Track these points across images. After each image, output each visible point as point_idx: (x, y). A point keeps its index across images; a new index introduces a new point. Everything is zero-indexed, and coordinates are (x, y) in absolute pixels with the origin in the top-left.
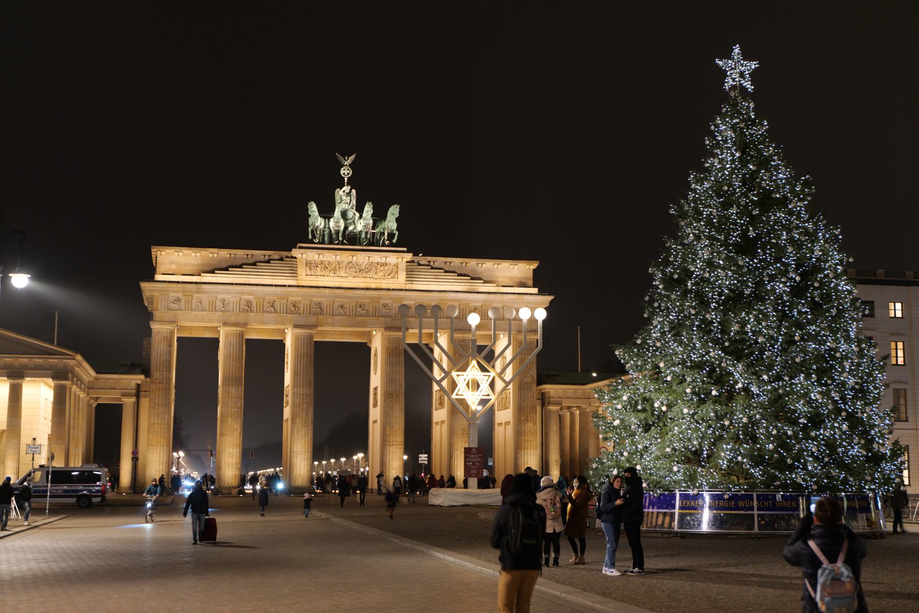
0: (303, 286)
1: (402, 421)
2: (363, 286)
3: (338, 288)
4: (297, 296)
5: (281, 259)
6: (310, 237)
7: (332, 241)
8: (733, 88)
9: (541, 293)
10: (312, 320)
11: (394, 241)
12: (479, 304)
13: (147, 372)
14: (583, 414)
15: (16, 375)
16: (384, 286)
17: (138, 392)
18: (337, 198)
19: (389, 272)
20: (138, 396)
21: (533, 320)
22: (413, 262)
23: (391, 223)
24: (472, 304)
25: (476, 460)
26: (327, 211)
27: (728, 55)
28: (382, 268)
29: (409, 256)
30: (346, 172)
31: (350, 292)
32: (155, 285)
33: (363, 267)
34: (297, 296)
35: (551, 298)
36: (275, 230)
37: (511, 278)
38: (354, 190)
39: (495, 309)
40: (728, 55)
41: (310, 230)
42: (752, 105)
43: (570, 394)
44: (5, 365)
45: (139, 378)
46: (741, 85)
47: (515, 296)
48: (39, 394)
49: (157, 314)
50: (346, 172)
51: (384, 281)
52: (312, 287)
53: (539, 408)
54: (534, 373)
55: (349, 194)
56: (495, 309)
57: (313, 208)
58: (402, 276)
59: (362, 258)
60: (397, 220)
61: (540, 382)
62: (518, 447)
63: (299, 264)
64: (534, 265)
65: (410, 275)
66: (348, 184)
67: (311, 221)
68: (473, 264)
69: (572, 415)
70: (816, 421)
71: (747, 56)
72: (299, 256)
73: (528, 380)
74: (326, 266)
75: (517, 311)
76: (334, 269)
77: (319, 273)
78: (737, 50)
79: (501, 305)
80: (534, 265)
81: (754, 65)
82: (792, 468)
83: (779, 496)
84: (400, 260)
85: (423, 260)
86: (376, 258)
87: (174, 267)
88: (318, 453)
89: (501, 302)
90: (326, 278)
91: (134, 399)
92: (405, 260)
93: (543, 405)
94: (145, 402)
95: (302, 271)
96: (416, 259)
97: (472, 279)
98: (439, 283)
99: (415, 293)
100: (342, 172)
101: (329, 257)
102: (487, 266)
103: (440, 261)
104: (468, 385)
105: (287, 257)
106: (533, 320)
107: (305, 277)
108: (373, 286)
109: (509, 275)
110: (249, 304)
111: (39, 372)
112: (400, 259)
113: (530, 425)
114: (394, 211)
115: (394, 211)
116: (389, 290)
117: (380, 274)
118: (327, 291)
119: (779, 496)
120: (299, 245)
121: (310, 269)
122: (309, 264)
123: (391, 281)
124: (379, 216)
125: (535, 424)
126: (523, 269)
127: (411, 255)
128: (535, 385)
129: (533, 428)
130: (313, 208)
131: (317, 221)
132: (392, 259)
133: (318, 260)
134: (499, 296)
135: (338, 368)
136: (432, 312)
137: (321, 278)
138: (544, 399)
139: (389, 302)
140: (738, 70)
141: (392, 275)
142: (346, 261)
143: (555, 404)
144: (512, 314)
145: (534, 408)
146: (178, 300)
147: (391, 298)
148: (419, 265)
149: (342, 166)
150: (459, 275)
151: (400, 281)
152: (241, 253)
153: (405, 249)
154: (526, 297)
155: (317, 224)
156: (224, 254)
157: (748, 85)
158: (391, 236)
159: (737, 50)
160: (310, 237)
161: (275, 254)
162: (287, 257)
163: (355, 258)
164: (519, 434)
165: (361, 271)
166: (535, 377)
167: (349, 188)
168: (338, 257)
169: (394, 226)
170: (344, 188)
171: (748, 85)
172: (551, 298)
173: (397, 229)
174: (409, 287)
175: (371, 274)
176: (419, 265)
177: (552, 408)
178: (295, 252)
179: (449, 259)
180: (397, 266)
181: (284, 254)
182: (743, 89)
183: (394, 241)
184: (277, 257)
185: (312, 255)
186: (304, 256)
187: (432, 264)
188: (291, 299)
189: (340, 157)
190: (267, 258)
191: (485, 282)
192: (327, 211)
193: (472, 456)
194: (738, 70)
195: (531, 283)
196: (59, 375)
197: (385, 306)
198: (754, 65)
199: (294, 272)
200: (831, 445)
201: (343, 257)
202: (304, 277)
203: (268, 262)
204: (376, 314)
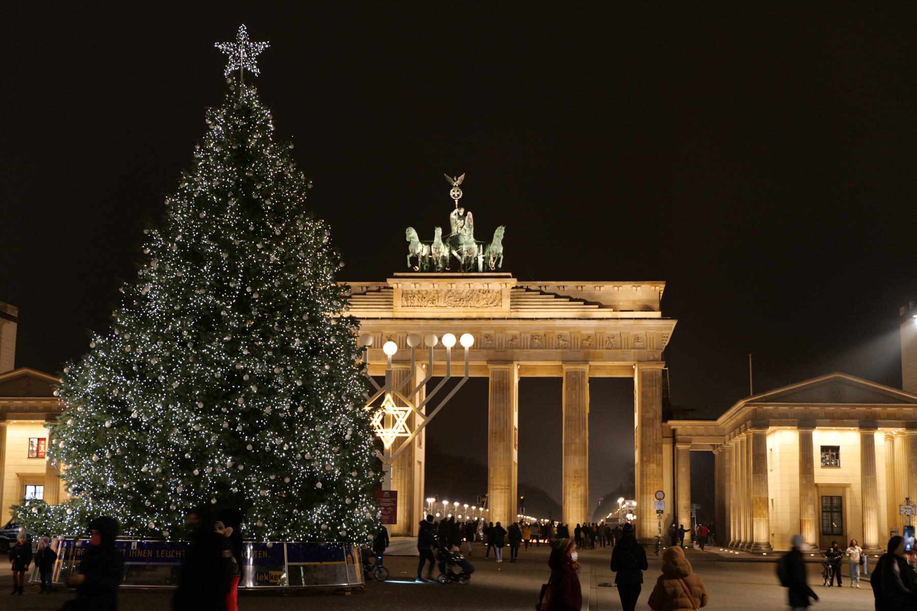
0: (397, 319)
2: (463, 315)
3: (434, 319)
4: (391, 329)
5: (379, 291)
6: (409, 265)
7: (430, 267)
8: (235, 73)
9: (664, 317)
11: (500, 266)
12: (592, 332)
16: (486, 315)
18: (452, 222)
21: (458, 347)
22: (522, 287)
23: (497, 247)
24: (583, 332)
25: (389, 505)
26: (427, 238)
27: (232, 37)
28: (484, 296)
29: (513, 282)
30: (455, 194)
31: (447, 322)
33: (464, 295)
34: (391, 329)
35: (673, 323)
37: (634, 302)
38: (469, 213)
39: (413, 336)
40: (232, 37)
41: (408, 257)
42: (253, 92)
43: (701, 430)
44: (45, 408)
46: (245, 69)
47: (631, 322)
50: (455, 194)
51: (486, 310)
52: (406, 319)
53: (667, 449)
54: (658, 408)
55: (460, 217)
56: (413, 336)
57: (412, 234)
58: (506, 303)
59: (462, 286)
60: (503, 242)
61: (667, 415)
63: (395, 295)
64: (660, 287)
65: (516, 301)
66: (459, 207)
67: (410, 248)
68: (589, 287)
70: (202, 455)
71: (254, 36)
72: (395, 286)
73: (650, 415)
74: (423, 296)
75: (440, 339)
76: (433, 299)
77: (416, 303)
78: (243, 30)
79: (617, 332)
80: (660, 287)
81: (263, 46)
82: (151, 512)
83: (134, 544)
84: (504, 286)
85: (534, 285)
86: (478, 285)
89: (616, 328)
90: (423, 309)
92: (510, 286)
93: (674, 442)
95: (398, 302)
96: (526, 284)
97: (586, 303)
98: (552, 312)
99: (517, 322)
100: (452, 193)
101: (426, 285)
103: (552, 286)
104: (395, 421)
105: (385, 288)
106: (458, 347)
107: (401, 309)
108: (474, 315)
109: (632, 298)
112: (507, 285)
113: (653, 466)
114: (500, 233)
115: (500, 233)
116: (489, 319)
117: (483, 303)
118: (422, 322)
119: (134, 544)
120: (395, 274)
121: (407, 300)
122: (405, 295)
123: (494, 309)
125: (660, 464)
126: (651, 291)
127: (515, 280)
128: (658, 422)
130: (412, 234)
131: (420, 249)
132: (495, 285)
133: (415, 290)
134: (612, 322)
137: (418, 309)
138: (673, 436)
139: (492, 332)
140: (243, 53)
141: (495, 303)
142: (445, 290)
143: (684, 442)
144: (432, 341)
147: (492, 328)
148: (528, 290)
149: (452, 187)
150: (572, 300)
153: (510, 274)
154: (644, 322)
155: (417, 252)
157: (256, 71)
159: (243, 30)
160: (409, 265)
161: (373, 285)
162: (385, 288)
163: (454, 286)
165: (460, 299)
166: (660, 412)
167: (462, 210)
168: (436, 286)
169: (501, 250)
170: (456, 211)
171: (256, 71)
173: (504, 253)
174: (514, 315)
175: (472, 303)
176: (528, 290)
177: (680, 446)
178: (391, 282)
179: (561, 283)
180: (500, 292)
181: (381, 284)
182: (248, 75)
183: (500, 266)
184: (376, 289)
185: (408, 285)
186: (400, 285)
187: (543, 289)
190: (365, 289)
191: (601, 306)
192: (427, 238)
193: (384, 500)
194: (243, 53)
195: (657, 306)
197: (487, 336)
198: (263, 46)
199: (389, 303)
200: (222, 485)
201: (442, 285)
202: (400, 308)
203: (364, 294)
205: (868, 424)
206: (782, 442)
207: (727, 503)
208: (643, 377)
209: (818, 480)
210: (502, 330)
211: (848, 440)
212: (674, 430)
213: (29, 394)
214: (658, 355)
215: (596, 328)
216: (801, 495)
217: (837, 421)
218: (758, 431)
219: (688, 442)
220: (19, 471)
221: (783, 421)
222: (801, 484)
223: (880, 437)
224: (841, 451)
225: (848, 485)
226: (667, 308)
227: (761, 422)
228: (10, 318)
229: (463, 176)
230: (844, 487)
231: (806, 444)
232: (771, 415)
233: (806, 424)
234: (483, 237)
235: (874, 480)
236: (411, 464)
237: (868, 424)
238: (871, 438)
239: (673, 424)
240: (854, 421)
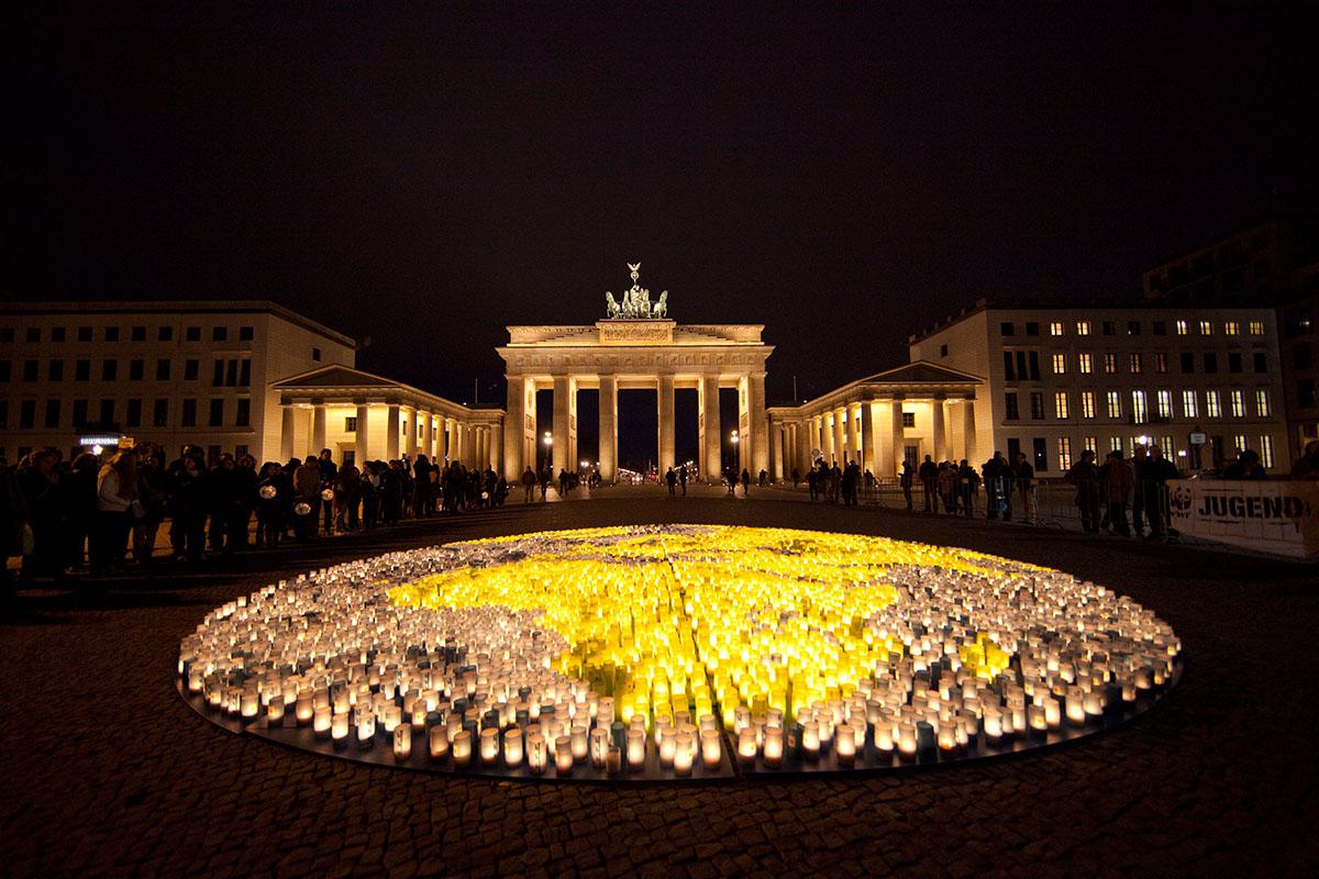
1: (673, 431)
7: (626, 318)
9: (766, 344)
10: (611, 369)
12: (723, 354)
13: (505, 409)
14: (798, 426)
15: (360, 400)
17: (502, 421)
19: (662, 337)
20: (502, 424)
26: (619, 299)
30: (635, 275)
32: (504, 349)
36: (588, 313)
45: (498, 412)
48: (378, 415)
49: (508, 369)
50: (635, 275)
53: (767, 424)
57: (610, 296)
58: (670, 337)
59: (642, 327)
61: (767, 406)
62: (753, 451)
65: (675, 336)
68: (719, 327)
69: (791, 429)
73: (758, 405)
74: (618, 333)
76: (623, 334)
80: (762, 328)
86: (652, 326)
87: (521, 340)
88: (623, 461)
91: (496, 425)
93: (770, 422)
94: (506, 427)
95: (603, 337)
102: (729, 329)
107: (604, 340)
110: (568, 359)
111: (377, 398)
114: (664, 295)
115: (664, 295)
124: (654, 298)
129: (763, 438)
130: (610, 296)
132: (663, 326)
135: (638, 406)
136: (693, 361)
138: (770, 418)
143: (778, 420)
145: (763, 423)
146: (522, 360)
151: (669, 341)
152: (564, 328)
156: (553, 329)
158: (663, 313)
161: (587, 328)
164: (753, 441)
165: (640, 334)
172: (773, 348)
178: (598, 325)
180: (666, 331)
181: (592, 327)
185: (609, 326)
188: (595, 356)
189: (630, 266)
192: (619, 299)
196: (393, 400)
199: (597, 337)
201: (631, 326)
204: (650, 364)
205: (940, 396)
206: (882, 411)
207: (805, 455)
208: (752, 383)
209: (906, 436)
210: (669, 353)
211: (921, 409)
212: (770, 415)
213: (341, 383)
214: (763, 368)
215: (728, 352)
216: (895, 445)
217: (919, 394)
218: (866, 402)
219: (781, 420)
220: (339, 441)
221: (883, 394)
222: (894, 438)
223: (945, 403)
224: (916, 416)
225: (921, 439)
226: (765, 337)
227: (867, 397)
228: (349, 346)
229: (638, 265)
230: (918, 440)
231: (898, 408)
232: (875, 392)
233: (899, 396)
234: (654, 298)
235: (944, 434)
236: (613, 437)
237: (940, 396)
238: (941, 405)
239: (773, 410)
240: (932, 395)
